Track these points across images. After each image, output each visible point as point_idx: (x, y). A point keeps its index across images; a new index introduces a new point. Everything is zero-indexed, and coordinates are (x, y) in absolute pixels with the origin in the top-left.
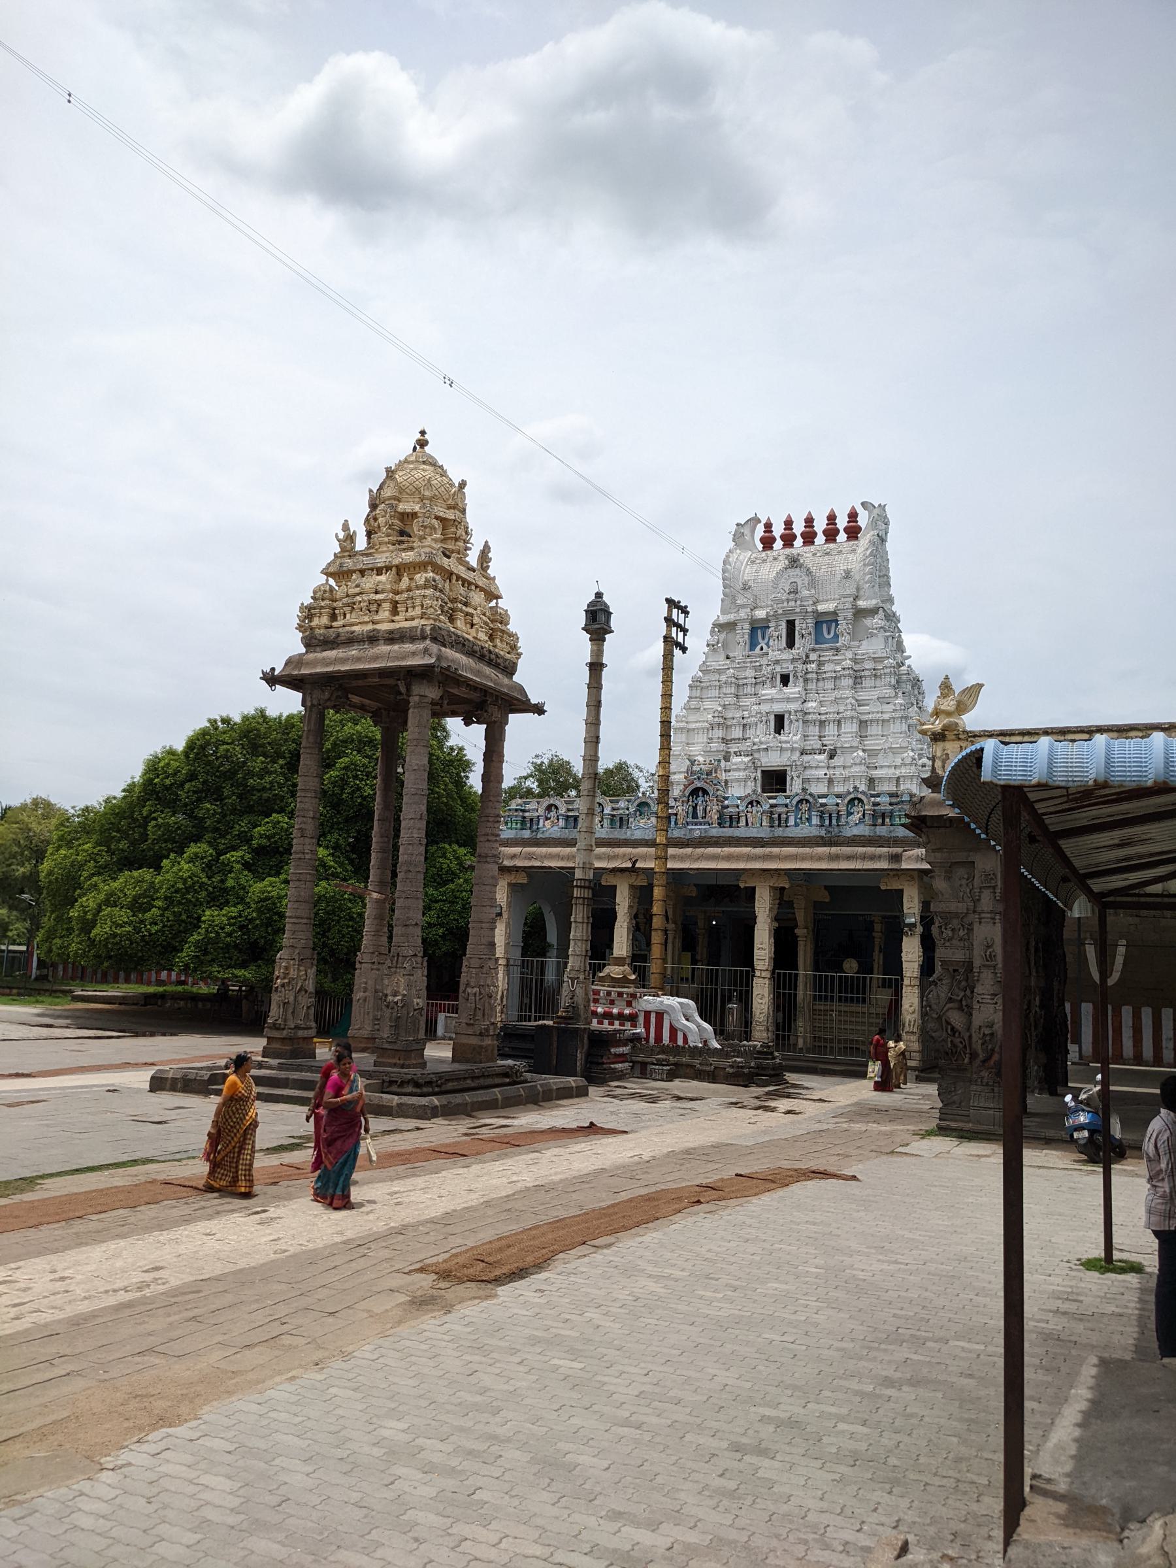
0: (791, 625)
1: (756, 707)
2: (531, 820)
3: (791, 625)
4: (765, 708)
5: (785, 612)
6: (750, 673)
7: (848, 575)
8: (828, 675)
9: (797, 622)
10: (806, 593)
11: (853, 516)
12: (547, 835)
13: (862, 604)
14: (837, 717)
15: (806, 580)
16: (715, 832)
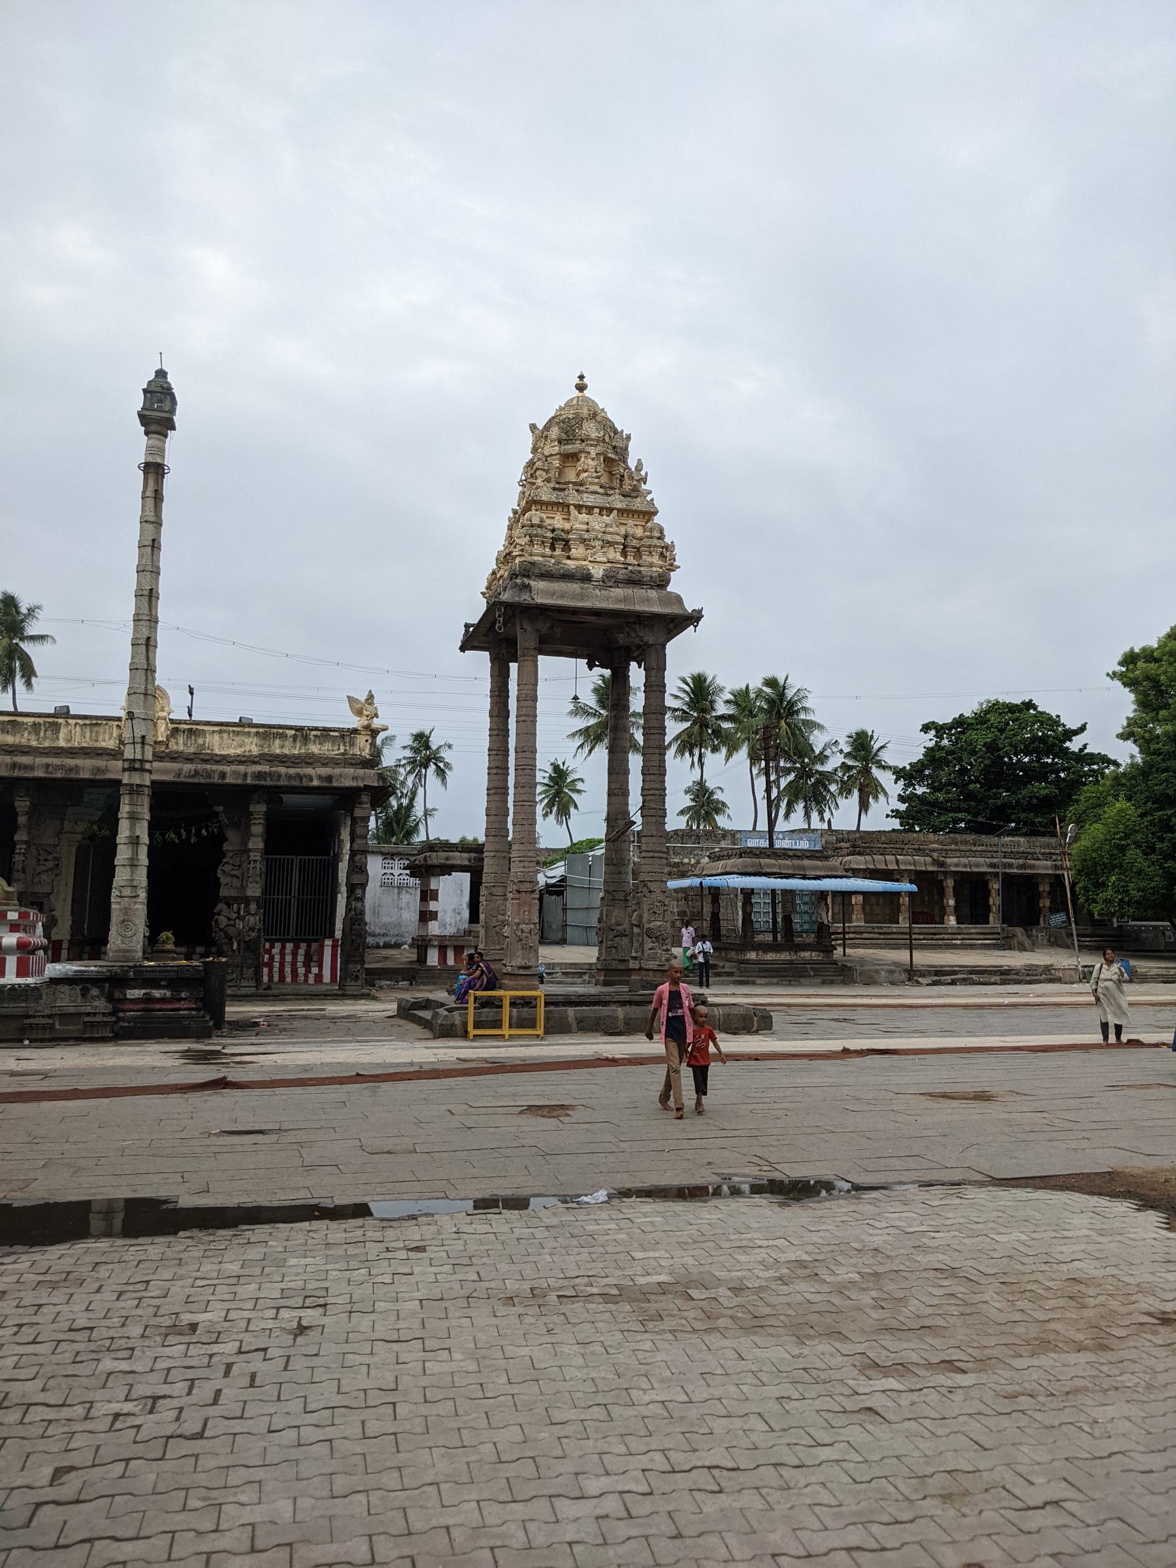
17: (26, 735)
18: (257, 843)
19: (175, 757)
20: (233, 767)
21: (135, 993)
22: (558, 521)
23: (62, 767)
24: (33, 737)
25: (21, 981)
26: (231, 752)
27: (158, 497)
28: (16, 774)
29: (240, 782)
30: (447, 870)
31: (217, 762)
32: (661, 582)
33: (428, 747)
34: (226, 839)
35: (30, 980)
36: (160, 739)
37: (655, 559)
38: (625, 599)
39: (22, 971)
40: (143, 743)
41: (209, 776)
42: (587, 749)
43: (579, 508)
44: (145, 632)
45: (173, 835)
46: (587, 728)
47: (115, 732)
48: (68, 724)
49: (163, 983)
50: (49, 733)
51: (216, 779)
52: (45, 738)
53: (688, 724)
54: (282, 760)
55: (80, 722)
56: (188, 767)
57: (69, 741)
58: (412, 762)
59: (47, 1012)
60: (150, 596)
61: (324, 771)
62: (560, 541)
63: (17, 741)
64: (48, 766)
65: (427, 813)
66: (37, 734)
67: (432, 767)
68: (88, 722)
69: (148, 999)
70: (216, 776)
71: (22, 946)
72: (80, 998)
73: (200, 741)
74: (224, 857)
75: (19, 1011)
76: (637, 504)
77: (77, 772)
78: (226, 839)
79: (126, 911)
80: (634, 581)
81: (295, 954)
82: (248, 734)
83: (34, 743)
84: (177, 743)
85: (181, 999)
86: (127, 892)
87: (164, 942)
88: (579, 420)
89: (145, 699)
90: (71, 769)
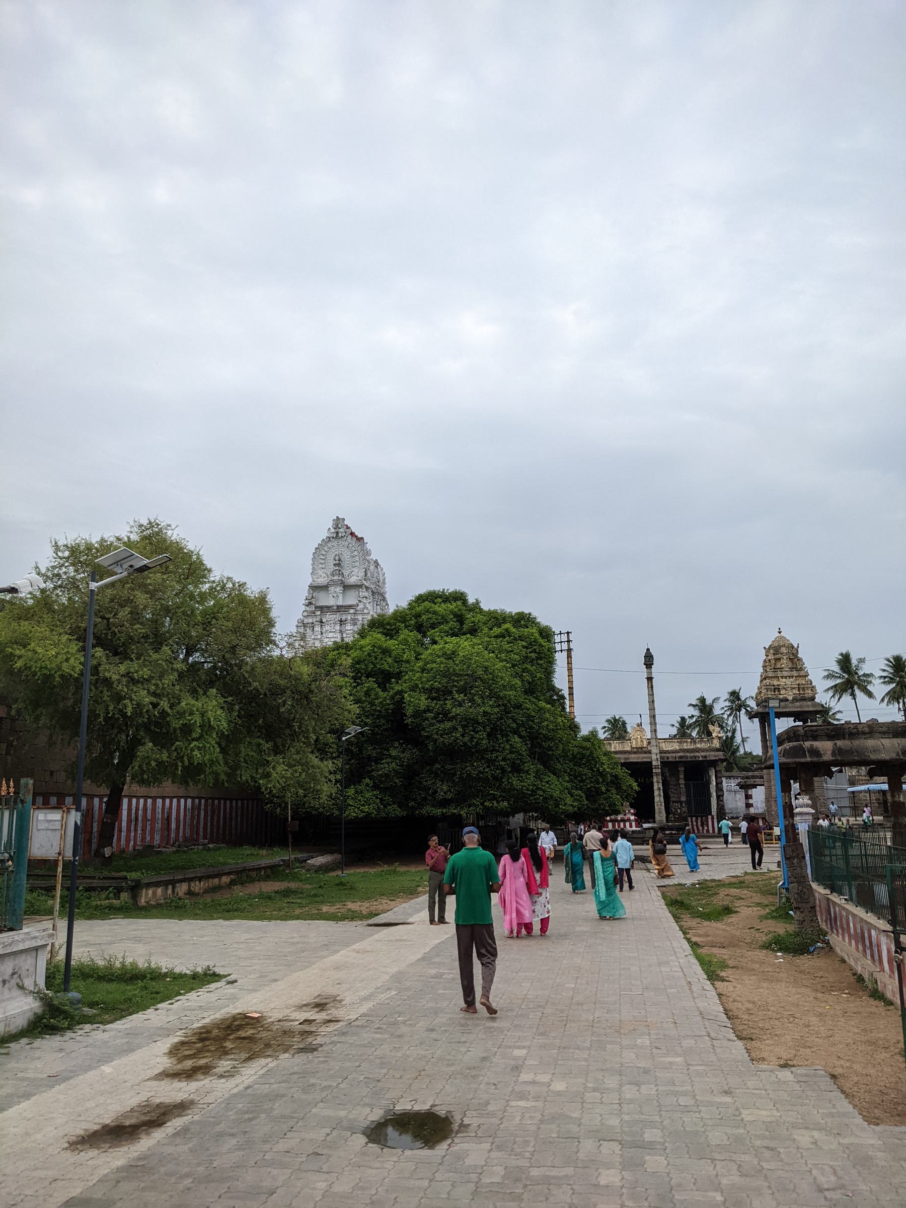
18: (682, 781)
21: (667, 832)
22: (776, 683)
27: (652, 687)
30: (755, 786)
32: (813, 699)
33: (739, 699)
37: (810, 691)
38: (800, 707)
42: (837, 697)
43: (782, 677)
46: (835, 686)
53: (894, 685)
54: (687, 751)
58: (731, 708)
61: (704, 754)
62: (777, 689)
65: (743, 740)
67: (743, 711)
69: (671, 834)
76: (802, 673)
80: (804, 699)
81: (697, 822)
88: (780, 647)
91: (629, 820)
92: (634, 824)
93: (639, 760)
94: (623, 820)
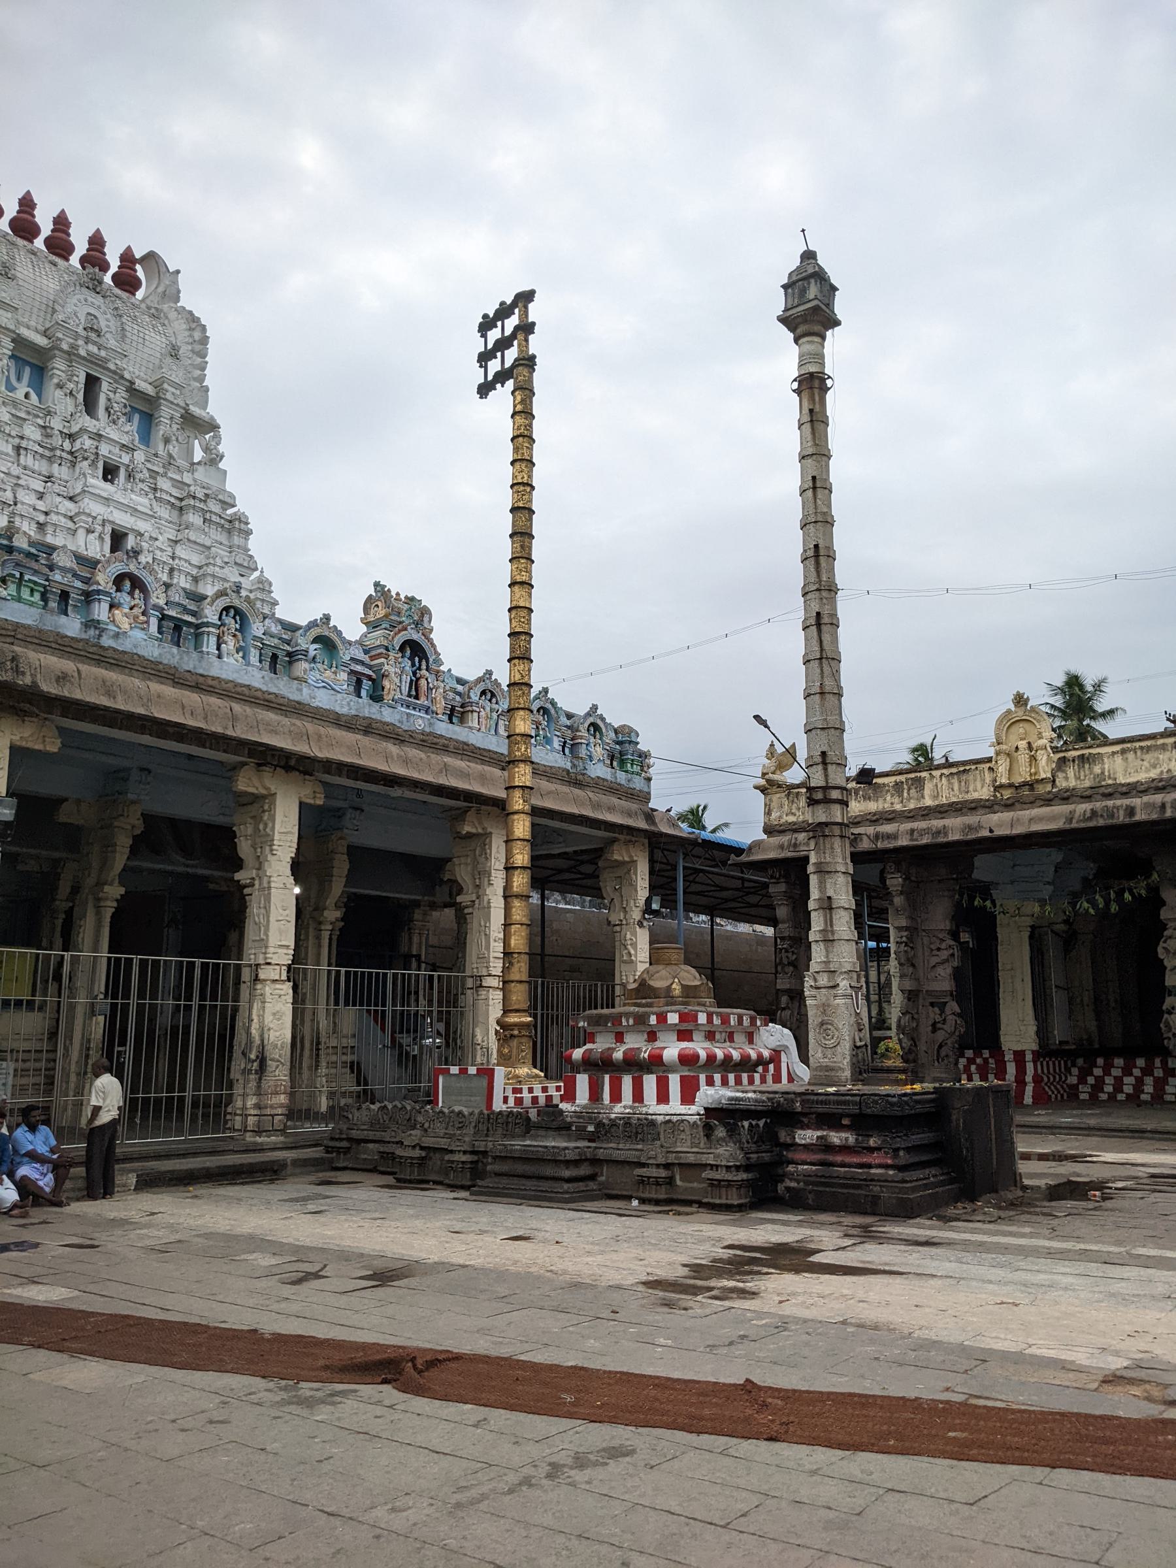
0: (92, 383)
1: (69, 505)
2: (64, 596)
3: (92, 383)
4: (96, 508)
5: (91, 360)
6: (32, 432)
7: (174, 353)
8: (164, 496)
9: (105, 386)
10: (112, 343)
11: (127, 258)
12: (125, 645)
13: (195, 410)
14: (194, 572)
15: (113, 323)
16: (443, 728)
17: (888, 798)
19: (1067, 797)
20: (1146, 799)
23: (927, 831)
24: (897, 800)
25: (683, 1109)
26: (1142, 776)
28: (880, 845)
29: (1154, 816)
31: (1125, 794)
34: (1163, 903)
35: (693, 1109)
36: (1043, 776)
39: (688, 1097)
40: (825, 763)
41: (1112, 816)
44: (815, 607)
45: (1086, 905)
47: (988, 777)
48: (932, 776)
49: (845, 1121)
50: (913, 791)
51: (1121, 818)
52: (909, 799)
55: (946, 771)
56: (1083, 808)
57: (936, 797)
59: (661, 1160)
60: (817, 556)
63: (881, 807)
64: (912, 831)
66: (901, 795)
68: (954, 770)
70: (1122, 813)
71: (687, 1060)
72: (703, 1140)
73: (1097, 769)
74: (1165, 929)
75: (631, 1156)
77: (946, 834)
78: (1163, 903)
79: (824, 1008)
82: (1163, 747)
83: (898, 807)
84: (1067, 778)
85: (871, 1150)
86: (823, 980)
87: (883, 1055)
89: (822, 699)
90: (938, 832)
91: (655, 1063)
92: (674, 1081)
93: (1018, 830)
94: (635, 1065)
